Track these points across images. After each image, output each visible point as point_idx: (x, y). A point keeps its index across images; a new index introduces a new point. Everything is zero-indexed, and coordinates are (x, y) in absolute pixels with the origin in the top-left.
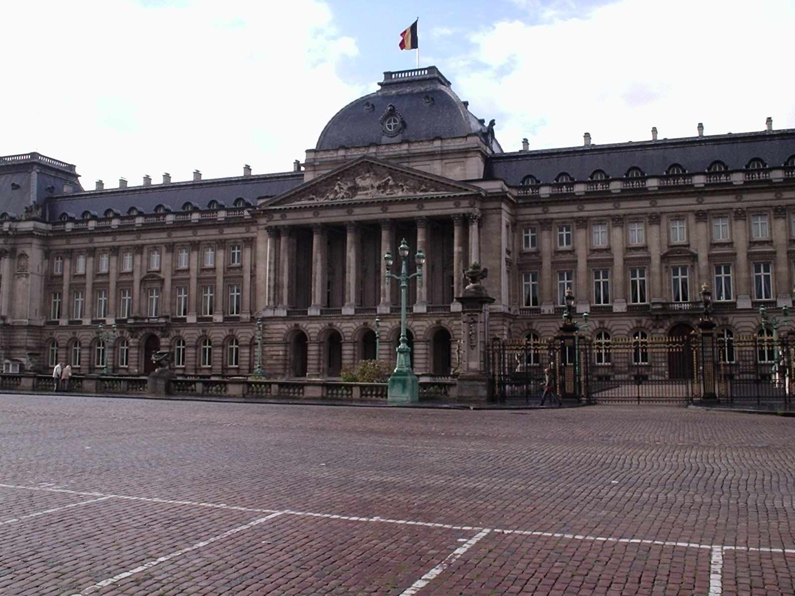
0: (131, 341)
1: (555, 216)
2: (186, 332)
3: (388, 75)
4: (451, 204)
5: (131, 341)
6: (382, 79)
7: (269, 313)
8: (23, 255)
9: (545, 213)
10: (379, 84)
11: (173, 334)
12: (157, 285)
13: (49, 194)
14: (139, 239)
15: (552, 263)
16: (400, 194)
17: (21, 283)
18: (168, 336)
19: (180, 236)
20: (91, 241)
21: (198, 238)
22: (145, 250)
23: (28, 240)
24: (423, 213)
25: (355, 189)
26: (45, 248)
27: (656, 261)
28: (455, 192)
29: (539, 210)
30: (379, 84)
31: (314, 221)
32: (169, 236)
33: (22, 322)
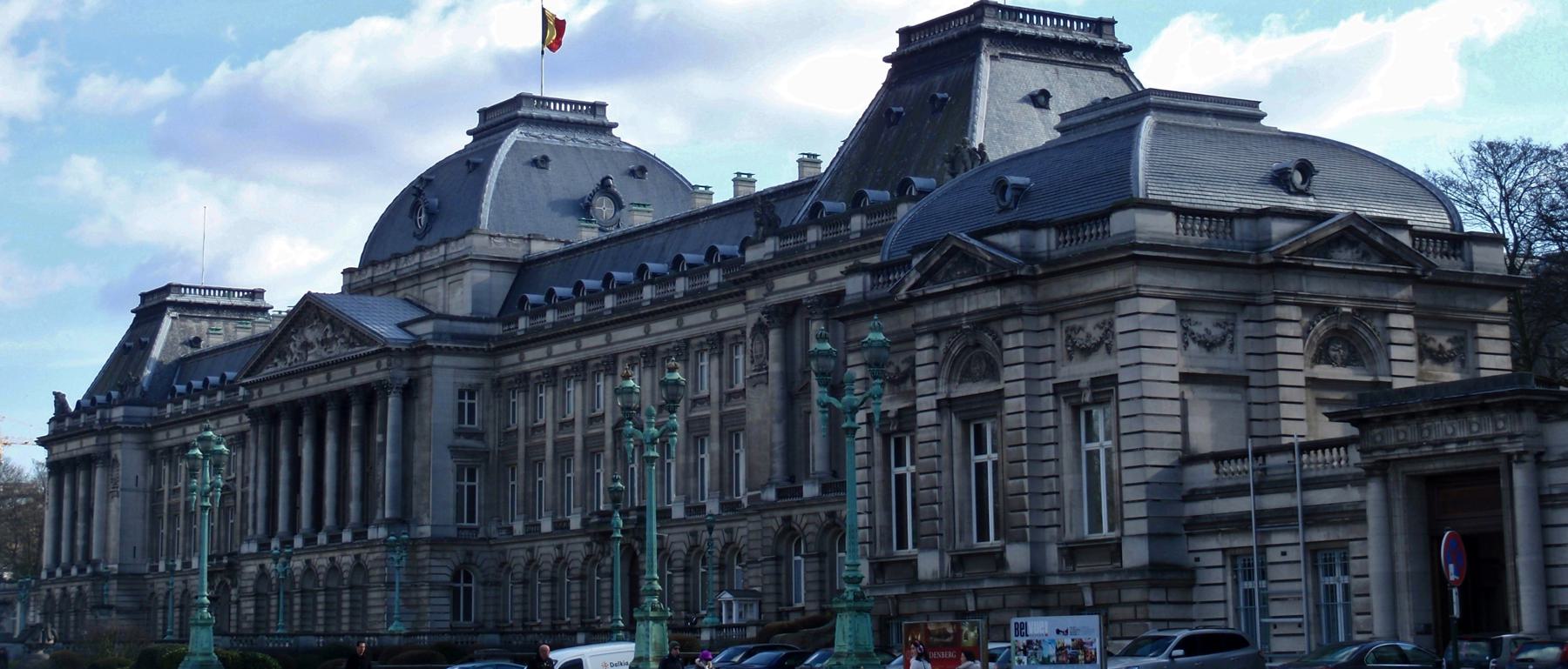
1: (527, 367)
3: (484, 113)
4: (371, 366)
6: (474, 123)
8: (116, 461)
9: (522, 361)
10: (469, 133)
13: (190, 351)
15: (527, 448)
17: (115, 504)
20: (184, 434)
23: (119, 437)
24: (355, 381)
25: (306, 346)
26: (150, 447)
27: (609, 441)
28: (369, 345)
29: (515, 358)
30: (469, 133)
31: (281, 399)
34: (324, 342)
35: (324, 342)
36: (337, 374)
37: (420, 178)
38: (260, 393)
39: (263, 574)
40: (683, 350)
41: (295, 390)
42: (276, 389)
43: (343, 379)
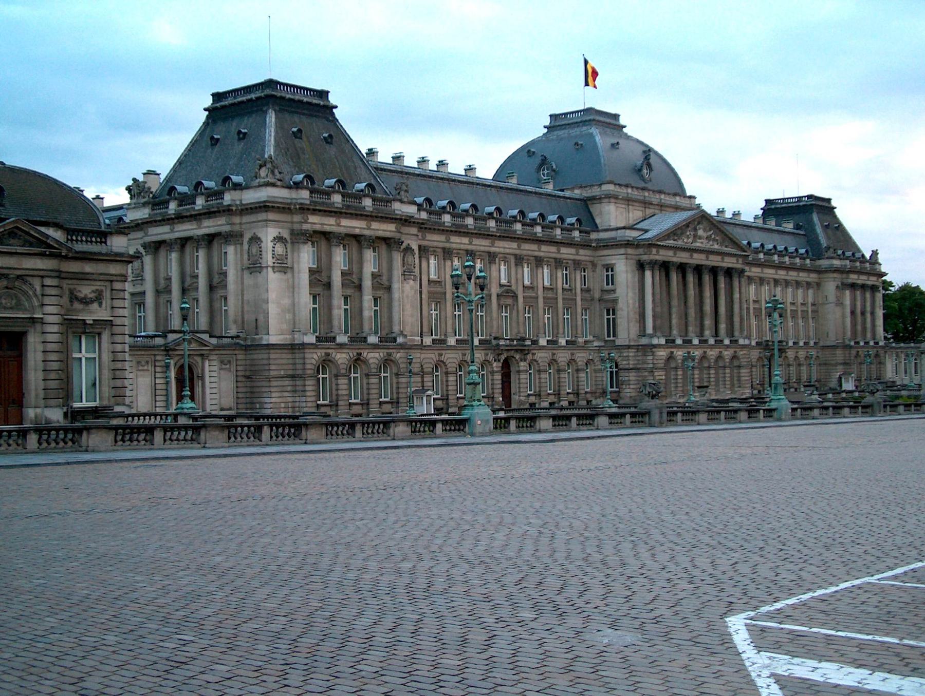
0: (495, 364)
2: (540, 355)
4: (734, 260)
5: (495, 364)
7: (655, 341)
11: (529, 357)
12: (509, 301)
14: (493, 246)
16: (716, 246)
18: (525, 360)
19: (529, 249)
21: (542, 254)
22: (497, 260)
31: (675, 260)
32: (519, 247)
33: (414, 340)
34: (708, 238)
35: (708, 238)
36: (712, 257)
37: (648, 152)
38: (658, 252)
39: (671, 357)
40: (787, 283)
41: (683, 258)
42: (671, 253)
43: (714, 261)
